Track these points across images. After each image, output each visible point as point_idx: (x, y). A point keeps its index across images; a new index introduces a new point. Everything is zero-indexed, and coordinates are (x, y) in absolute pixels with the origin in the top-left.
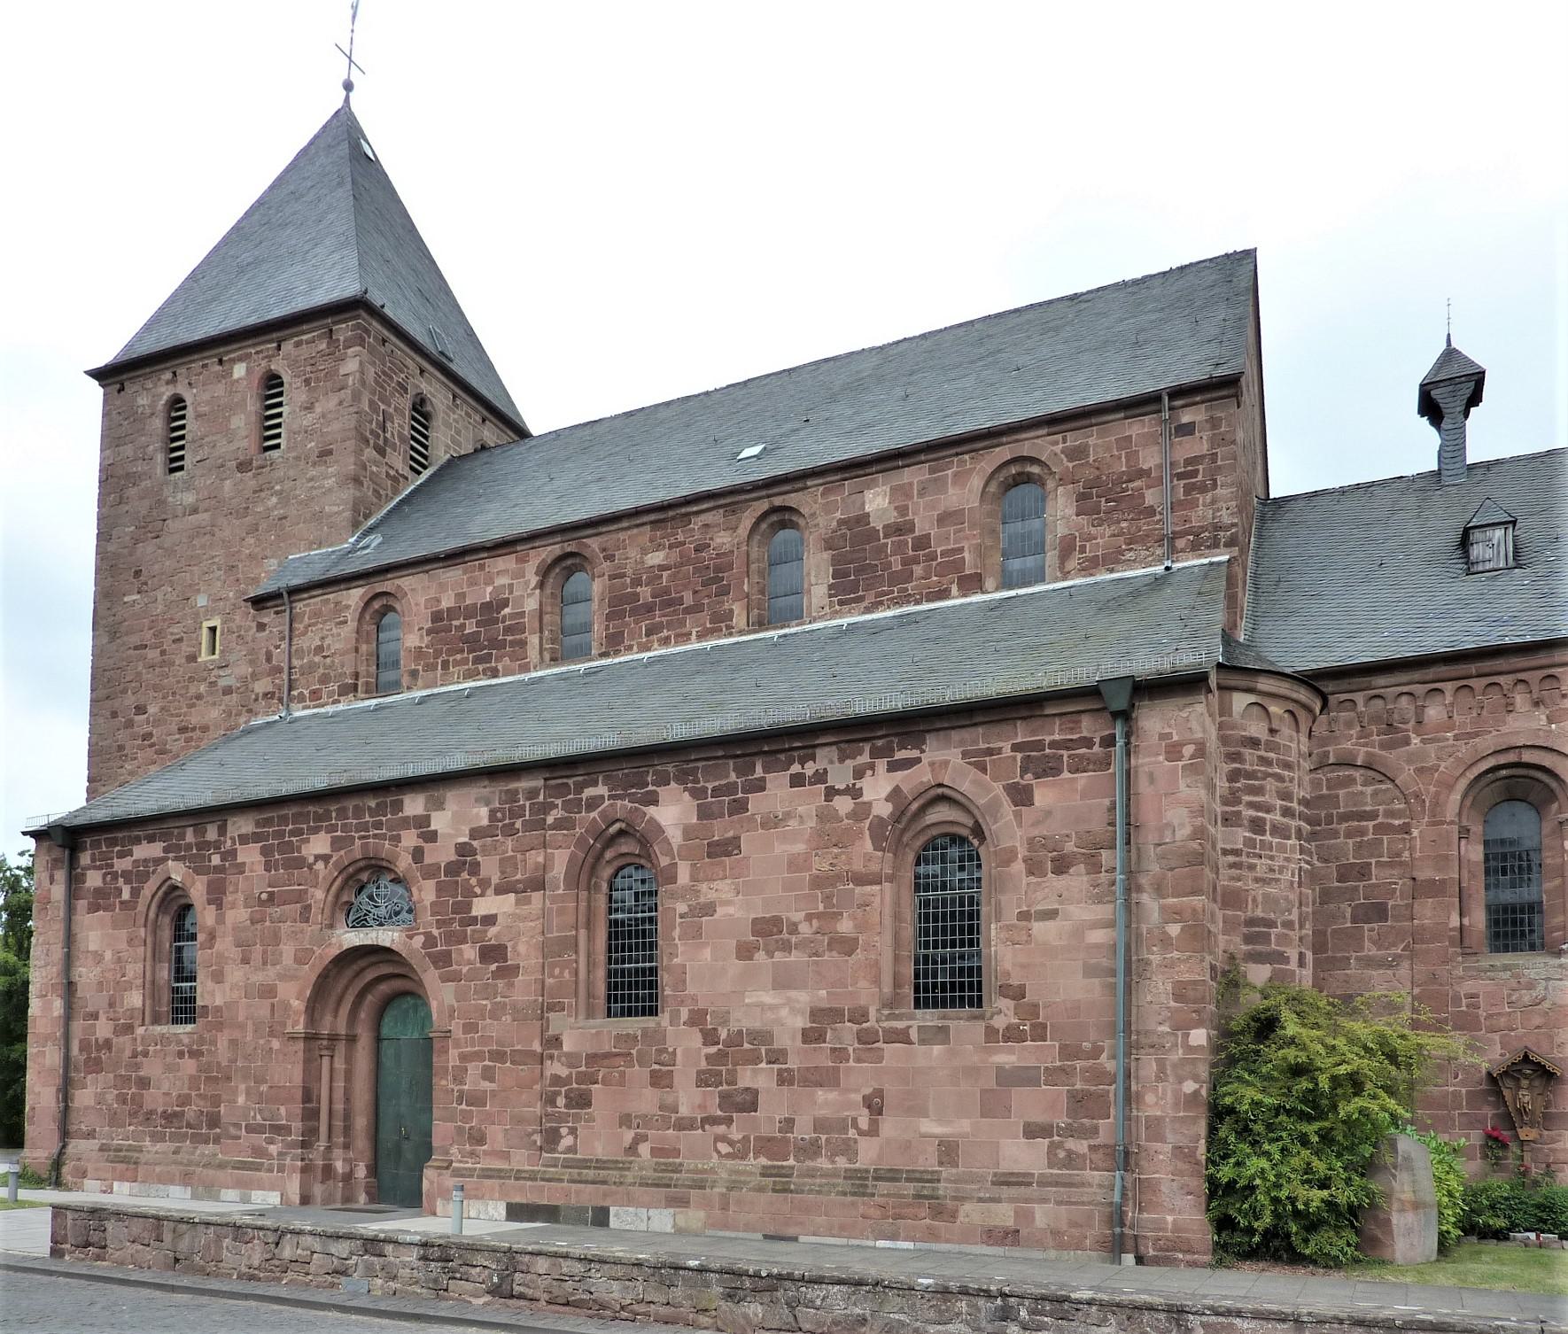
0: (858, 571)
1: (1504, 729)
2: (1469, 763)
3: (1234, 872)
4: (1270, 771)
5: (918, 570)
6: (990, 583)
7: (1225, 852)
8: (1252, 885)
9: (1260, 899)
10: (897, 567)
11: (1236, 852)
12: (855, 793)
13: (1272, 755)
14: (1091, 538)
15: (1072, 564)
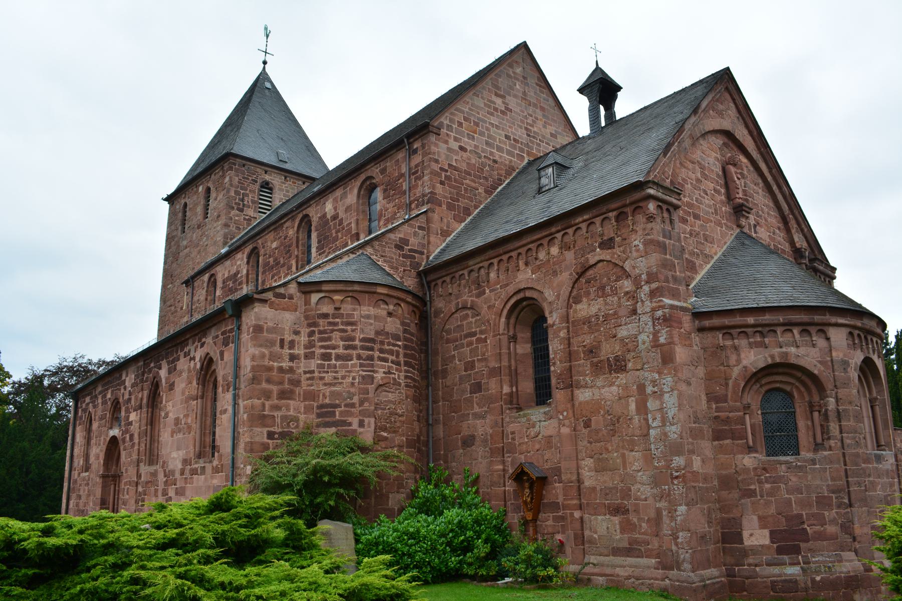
0: (324, 239)
1: (517, 280)
2: (505, 300)
3: (310, 382)
4: (336, 328)
5: (340, 235)
6: (362, 236)
7: (305, 373)
8: (322, 387)
9: (328, 394)
10: (334, 235)
11: (312, 372)
12: (193, 359)
13: (337, 320)
14: (387, 210)
15: (382, 223)
